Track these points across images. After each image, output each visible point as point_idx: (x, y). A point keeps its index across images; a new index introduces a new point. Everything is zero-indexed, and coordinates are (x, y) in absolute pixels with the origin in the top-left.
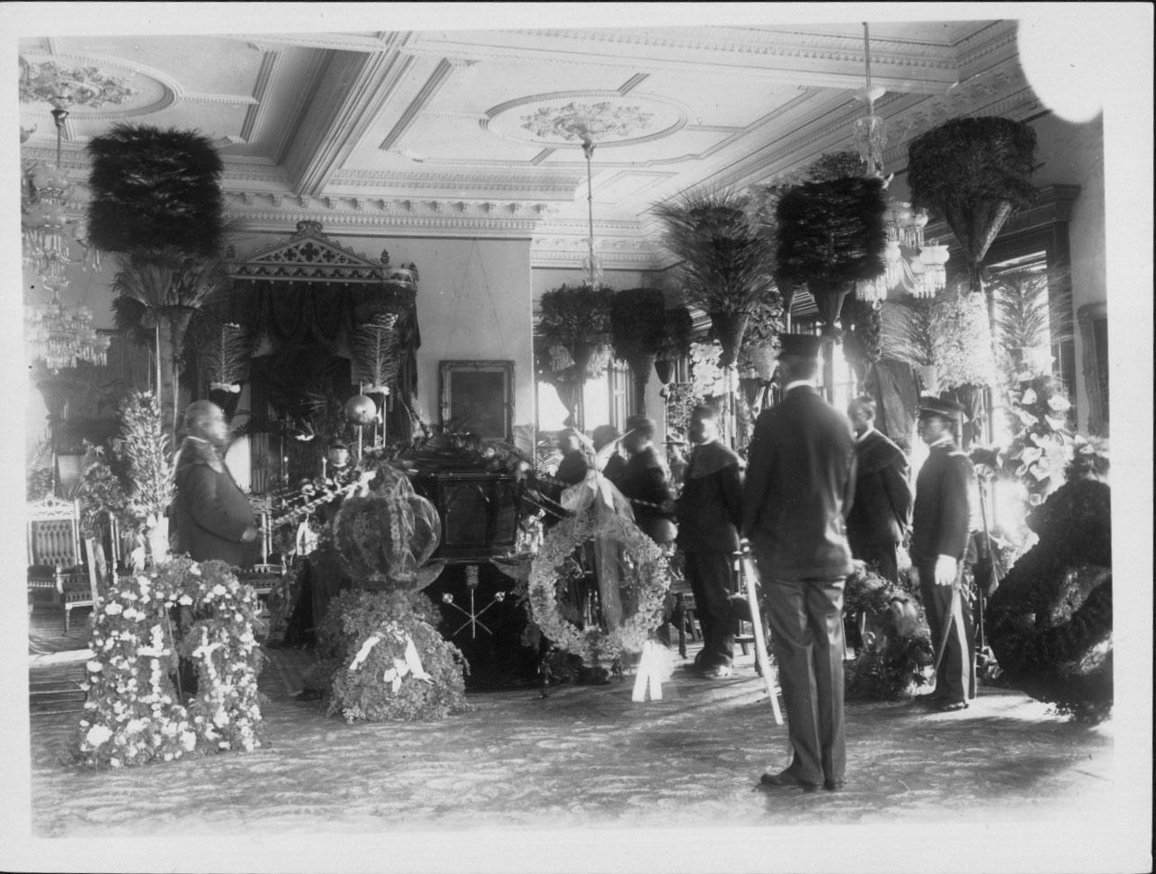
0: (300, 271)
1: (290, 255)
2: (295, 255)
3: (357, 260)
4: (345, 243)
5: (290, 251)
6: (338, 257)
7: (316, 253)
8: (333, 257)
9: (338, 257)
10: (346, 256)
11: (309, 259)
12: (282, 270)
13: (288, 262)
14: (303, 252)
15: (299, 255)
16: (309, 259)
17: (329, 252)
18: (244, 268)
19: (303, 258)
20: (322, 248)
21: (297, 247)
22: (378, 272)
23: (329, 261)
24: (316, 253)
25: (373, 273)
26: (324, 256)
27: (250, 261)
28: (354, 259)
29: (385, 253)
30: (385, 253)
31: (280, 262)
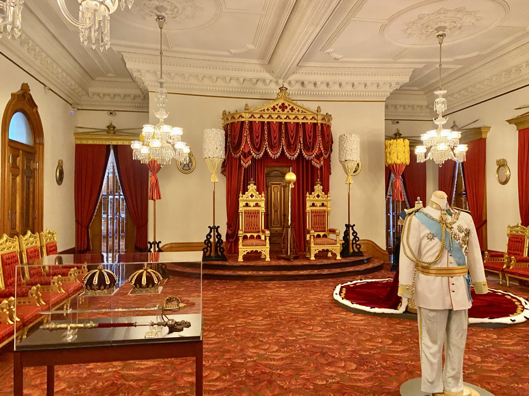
0: (279, 117)
1: (274, 109)
2: (276, 109)
3: (305, 111)
4: (299, 103)
5: (274, 107)
6: (296, 110)
7: (286, 107)
8: (294, 109)
9: (296, 110)
10: (300, 110)
11: (283, 111)
12: (270, 116)
13: (273, 112)
14: (280, 107)
15: (278, 109)
16: (283, 111)
17: (292, 107)
18: (252, 116)
19: (280, 110)
20: (289, 105)
21: (277, 105)
22: (316, 116)
23: (292, 111)
24: (286, 107)
26: (290, 109)
27: (254, 112)
28: (304, 110)
29: (319, 107)
30: (319, 107)
31: (269, 112)
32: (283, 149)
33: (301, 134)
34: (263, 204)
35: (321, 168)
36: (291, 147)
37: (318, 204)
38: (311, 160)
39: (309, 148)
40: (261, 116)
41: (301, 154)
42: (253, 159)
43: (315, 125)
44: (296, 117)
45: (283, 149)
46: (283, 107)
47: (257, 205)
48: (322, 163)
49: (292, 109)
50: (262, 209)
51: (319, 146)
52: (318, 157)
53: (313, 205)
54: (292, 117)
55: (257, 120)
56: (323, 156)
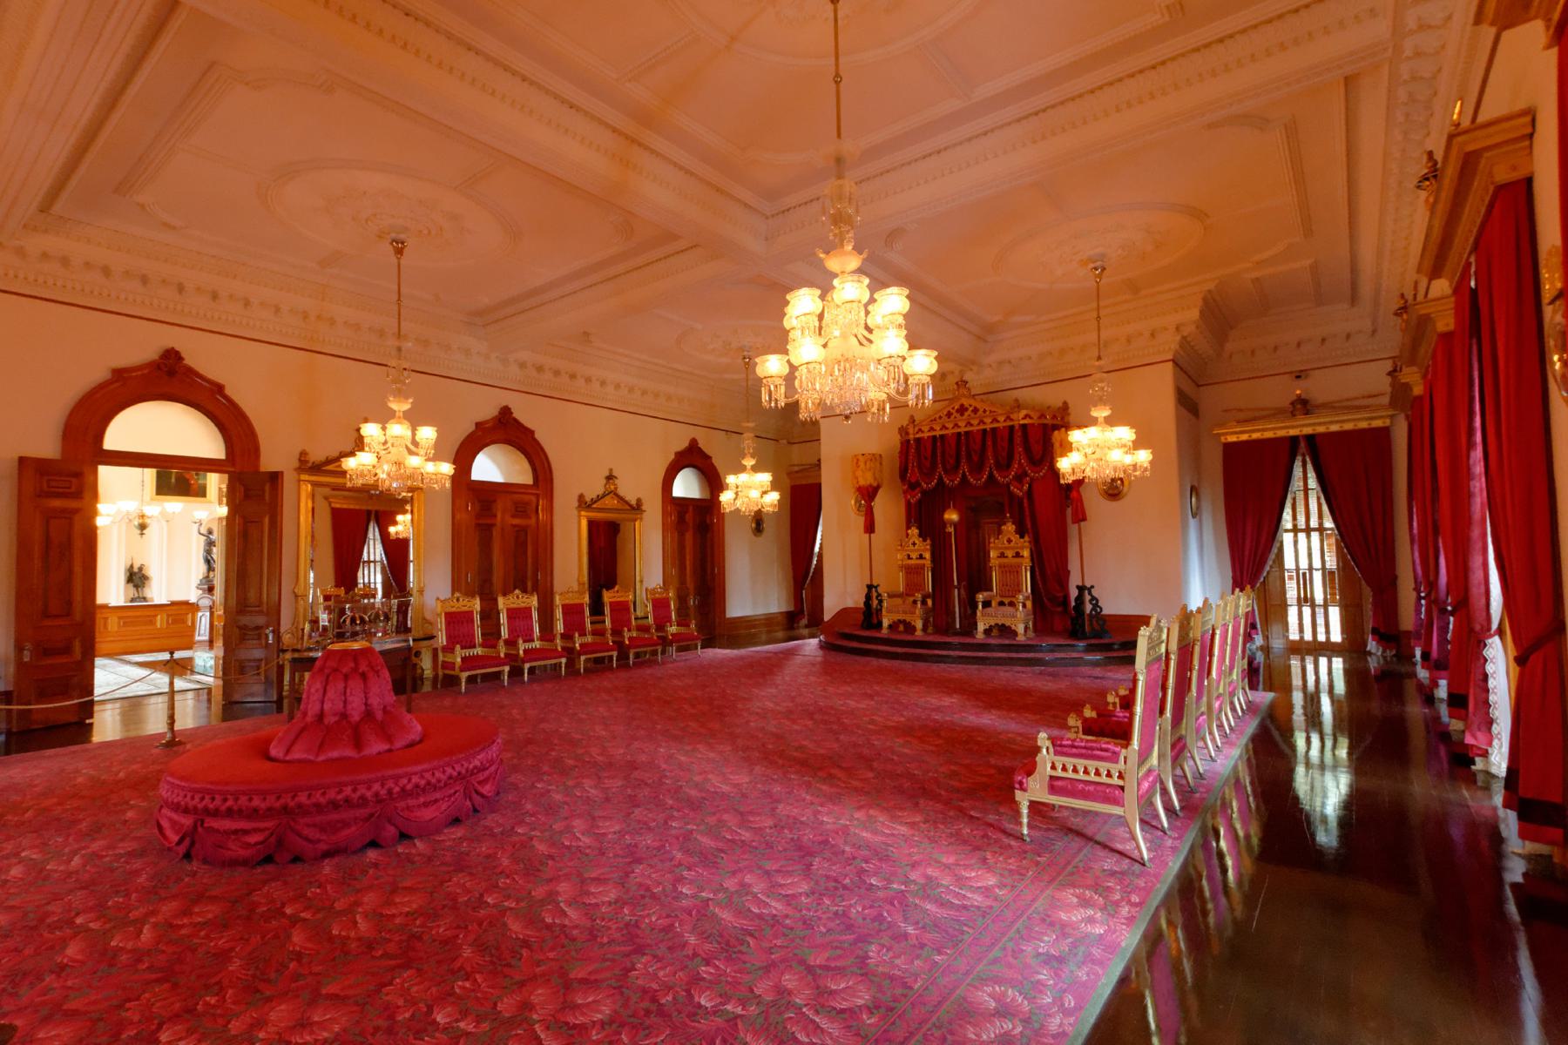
1: (949, 415)
25: (1008, 418)
32: (964, 474)
33: (989, 443)
34: (927, 555)
35: (1029, 493)
36: (977, 469)
37: (1010, 554)
38: (1008, 485)
39: (1004, 466)
40: (932, 429)
41: (991, 476)
42: (924, 493)
43: (1012, 427)
44: (982, 422)
45: (964, 474)
46: (962, 410)
47: (921, 557)
48: (1026, 487)
49: (976, 410)
50: (928, 562)
51: (1020, 460)
52: (1020, 478)
53: (1002, 555)
54: (975, 422)
55: (926, 435)
56: (1026, 475)
